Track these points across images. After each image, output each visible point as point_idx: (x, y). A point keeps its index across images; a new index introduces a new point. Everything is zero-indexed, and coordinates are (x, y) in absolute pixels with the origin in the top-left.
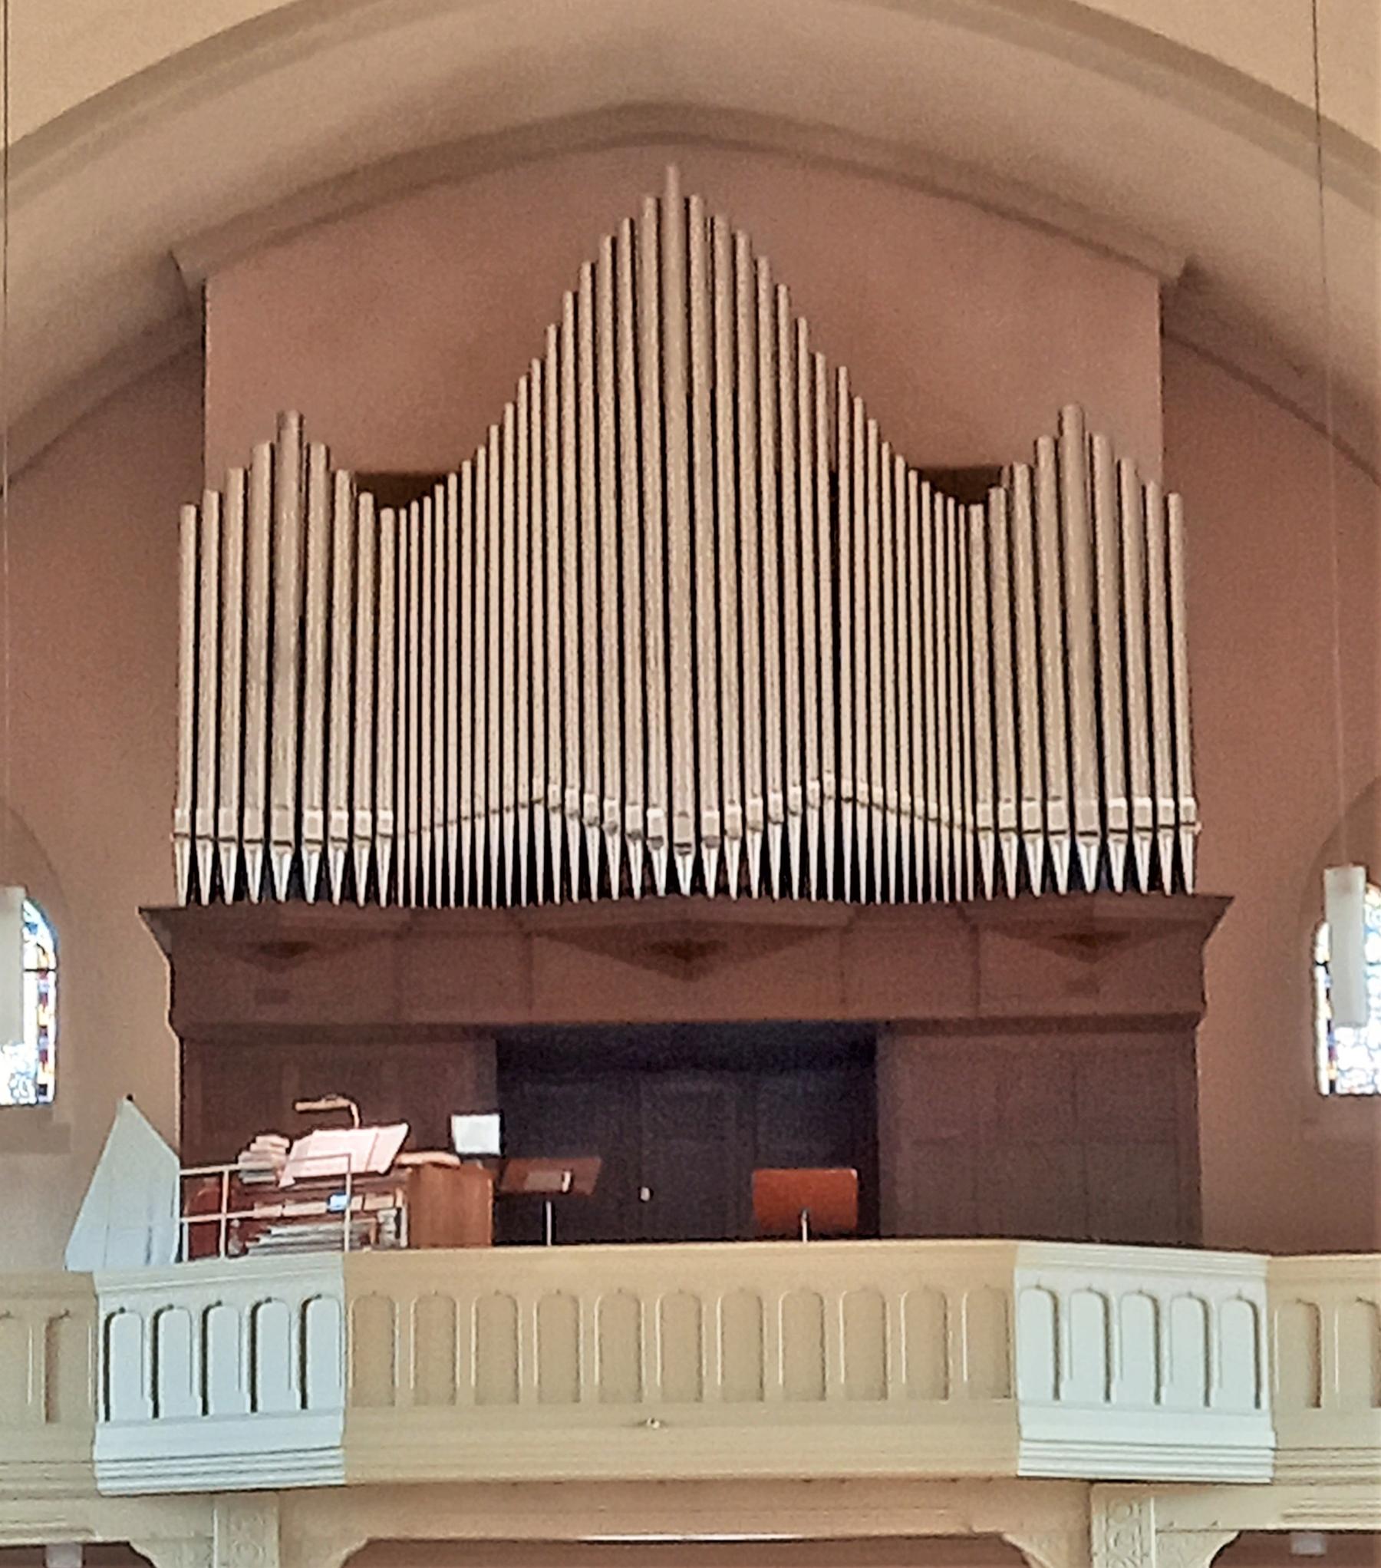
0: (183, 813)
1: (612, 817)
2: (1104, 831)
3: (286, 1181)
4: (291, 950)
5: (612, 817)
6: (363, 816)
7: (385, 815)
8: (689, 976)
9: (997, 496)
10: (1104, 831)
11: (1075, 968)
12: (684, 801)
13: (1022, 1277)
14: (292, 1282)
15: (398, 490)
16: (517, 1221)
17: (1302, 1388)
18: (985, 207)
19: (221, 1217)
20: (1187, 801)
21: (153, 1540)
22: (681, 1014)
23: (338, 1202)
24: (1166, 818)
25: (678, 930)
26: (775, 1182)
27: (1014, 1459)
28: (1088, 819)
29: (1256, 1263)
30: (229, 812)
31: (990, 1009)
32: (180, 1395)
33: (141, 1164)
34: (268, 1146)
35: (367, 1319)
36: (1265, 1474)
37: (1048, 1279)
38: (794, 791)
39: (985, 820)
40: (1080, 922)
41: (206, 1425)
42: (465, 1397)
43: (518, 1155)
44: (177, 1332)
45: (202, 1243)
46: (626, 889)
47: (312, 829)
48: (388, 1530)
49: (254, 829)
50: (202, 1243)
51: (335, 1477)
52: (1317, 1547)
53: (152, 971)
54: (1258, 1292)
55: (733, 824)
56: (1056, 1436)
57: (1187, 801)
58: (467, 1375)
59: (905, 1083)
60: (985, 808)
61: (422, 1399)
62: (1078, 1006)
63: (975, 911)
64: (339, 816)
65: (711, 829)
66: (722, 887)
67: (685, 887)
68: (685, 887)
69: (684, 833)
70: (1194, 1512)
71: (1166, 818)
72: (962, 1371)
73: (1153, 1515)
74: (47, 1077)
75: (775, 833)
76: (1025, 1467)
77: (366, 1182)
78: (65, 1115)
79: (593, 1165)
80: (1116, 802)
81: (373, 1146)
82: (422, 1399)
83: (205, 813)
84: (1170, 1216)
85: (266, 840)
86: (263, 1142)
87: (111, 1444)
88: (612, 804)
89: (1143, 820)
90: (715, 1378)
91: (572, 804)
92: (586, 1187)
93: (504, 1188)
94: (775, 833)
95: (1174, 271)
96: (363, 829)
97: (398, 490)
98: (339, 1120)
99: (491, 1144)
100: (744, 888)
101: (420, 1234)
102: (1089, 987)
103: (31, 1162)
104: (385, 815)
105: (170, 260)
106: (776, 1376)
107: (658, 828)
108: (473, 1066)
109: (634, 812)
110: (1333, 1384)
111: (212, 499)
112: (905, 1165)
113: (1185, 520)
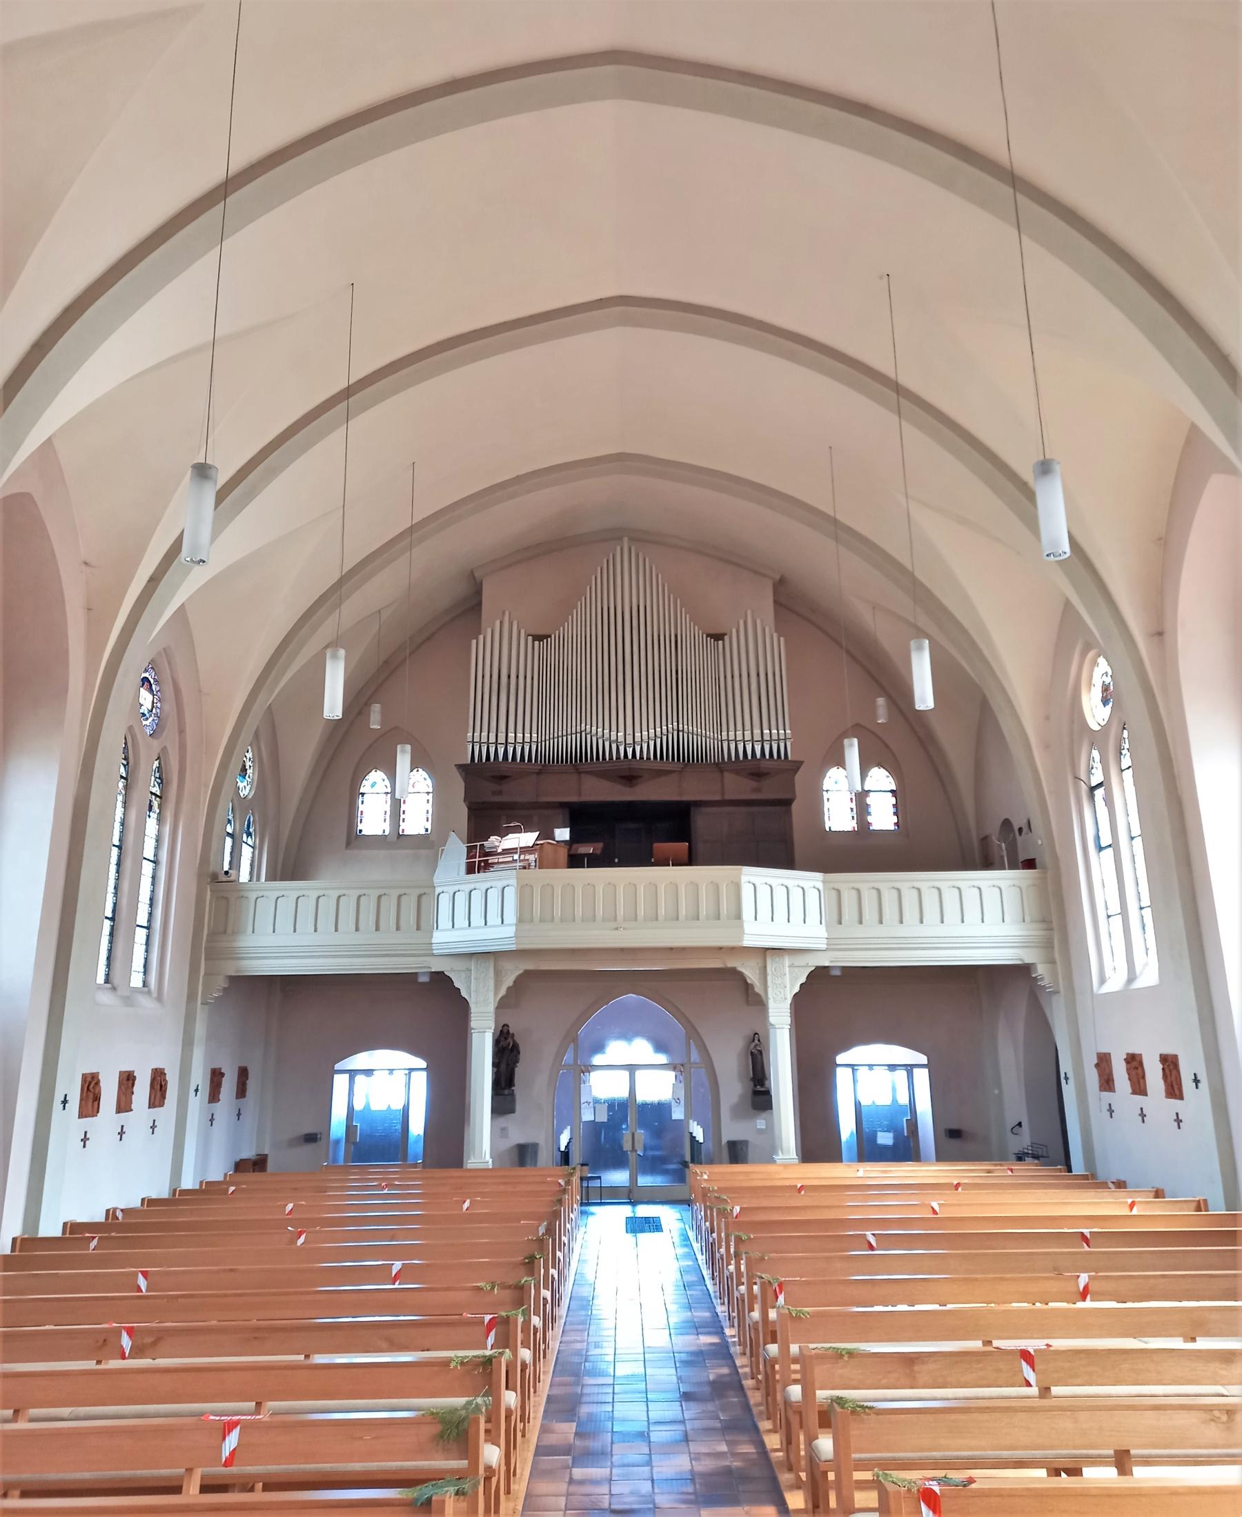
0: (470, 734)
1: (606, 736)
2: (763, 741)
3: (500, 850)
4: (502, 778)
5: (606, 736)
7: (534, 735)
8: (631, 786)
9: (726, 638)
10: (763, 741)
11: (754, 784)
12: (629, 731)
13: (744, 879)
14: (501, 886)
15: (539, 638)
16: (575, 861)
17: (835, 918)
18: (721, 559)
19: (479, 862)
20: (788, 731)
21: (452, 970)
23: (516, 857)
24: (782, 737)
25: (628, 772)
26: (660, 847)
27: (741, 939)
28: (757, 737)
30: (484, 734)
31: (727, 797)
32: (461, 920)
33: (456, 851)
34: (493, 839)
35: (524, 894)
36: (824, 947)
37: (753, 879)
40: (752, 769)
41: (469, 931)
42: (557, 919)
43: (578, 842)
44: (461, 899)
45: (470, 869)
46: (611, 758)
47: (511, 740)
48: (530, 966)
49: (492, 739)
50: (470, 869)
51: (513, 947)
52: (838, 973)
53: (458, 786)
54: (820, 885)
55: (645, 738)
56: (755, 933)
57: (788, 731)
58: (558, 912)
59: (701, 822)
60: (724, 734)
61: (542, 920)
63: (721, 767)
64: (520, 735)
65: (638, 739)
66: (641, 758)
67: (630, 756)
68: (630, 756)
69: (629, 740)
70: (800, 960)
71: (782, 737)
72: (724, 910)
73: (787, 961)
74: (429, 826)
75: (658, 741)
76: (747, 942)
77: (525, 850)
78: (432, 838)
79: (600, 845)
80: (766, 731)
81: (528, 838)
82: (542, 920)
87: (438, 937)
88: (607, 731)
89: (775, 737)
90: (641, 913)
91: (594, 731)
92: (598, 852)
93: (572, 852)
94: (658, 741)
97: (539, 638)
98: (517, 830)
99: (567, 837)
100: (648, 758)
101: (541, 864)
102: (758, 790)
103: (423, 852)
104: (534, 735)
106: (662, 912)
107: (621, 739)
108: (561, 815)
110: (846, 918)
112: (700, 847)
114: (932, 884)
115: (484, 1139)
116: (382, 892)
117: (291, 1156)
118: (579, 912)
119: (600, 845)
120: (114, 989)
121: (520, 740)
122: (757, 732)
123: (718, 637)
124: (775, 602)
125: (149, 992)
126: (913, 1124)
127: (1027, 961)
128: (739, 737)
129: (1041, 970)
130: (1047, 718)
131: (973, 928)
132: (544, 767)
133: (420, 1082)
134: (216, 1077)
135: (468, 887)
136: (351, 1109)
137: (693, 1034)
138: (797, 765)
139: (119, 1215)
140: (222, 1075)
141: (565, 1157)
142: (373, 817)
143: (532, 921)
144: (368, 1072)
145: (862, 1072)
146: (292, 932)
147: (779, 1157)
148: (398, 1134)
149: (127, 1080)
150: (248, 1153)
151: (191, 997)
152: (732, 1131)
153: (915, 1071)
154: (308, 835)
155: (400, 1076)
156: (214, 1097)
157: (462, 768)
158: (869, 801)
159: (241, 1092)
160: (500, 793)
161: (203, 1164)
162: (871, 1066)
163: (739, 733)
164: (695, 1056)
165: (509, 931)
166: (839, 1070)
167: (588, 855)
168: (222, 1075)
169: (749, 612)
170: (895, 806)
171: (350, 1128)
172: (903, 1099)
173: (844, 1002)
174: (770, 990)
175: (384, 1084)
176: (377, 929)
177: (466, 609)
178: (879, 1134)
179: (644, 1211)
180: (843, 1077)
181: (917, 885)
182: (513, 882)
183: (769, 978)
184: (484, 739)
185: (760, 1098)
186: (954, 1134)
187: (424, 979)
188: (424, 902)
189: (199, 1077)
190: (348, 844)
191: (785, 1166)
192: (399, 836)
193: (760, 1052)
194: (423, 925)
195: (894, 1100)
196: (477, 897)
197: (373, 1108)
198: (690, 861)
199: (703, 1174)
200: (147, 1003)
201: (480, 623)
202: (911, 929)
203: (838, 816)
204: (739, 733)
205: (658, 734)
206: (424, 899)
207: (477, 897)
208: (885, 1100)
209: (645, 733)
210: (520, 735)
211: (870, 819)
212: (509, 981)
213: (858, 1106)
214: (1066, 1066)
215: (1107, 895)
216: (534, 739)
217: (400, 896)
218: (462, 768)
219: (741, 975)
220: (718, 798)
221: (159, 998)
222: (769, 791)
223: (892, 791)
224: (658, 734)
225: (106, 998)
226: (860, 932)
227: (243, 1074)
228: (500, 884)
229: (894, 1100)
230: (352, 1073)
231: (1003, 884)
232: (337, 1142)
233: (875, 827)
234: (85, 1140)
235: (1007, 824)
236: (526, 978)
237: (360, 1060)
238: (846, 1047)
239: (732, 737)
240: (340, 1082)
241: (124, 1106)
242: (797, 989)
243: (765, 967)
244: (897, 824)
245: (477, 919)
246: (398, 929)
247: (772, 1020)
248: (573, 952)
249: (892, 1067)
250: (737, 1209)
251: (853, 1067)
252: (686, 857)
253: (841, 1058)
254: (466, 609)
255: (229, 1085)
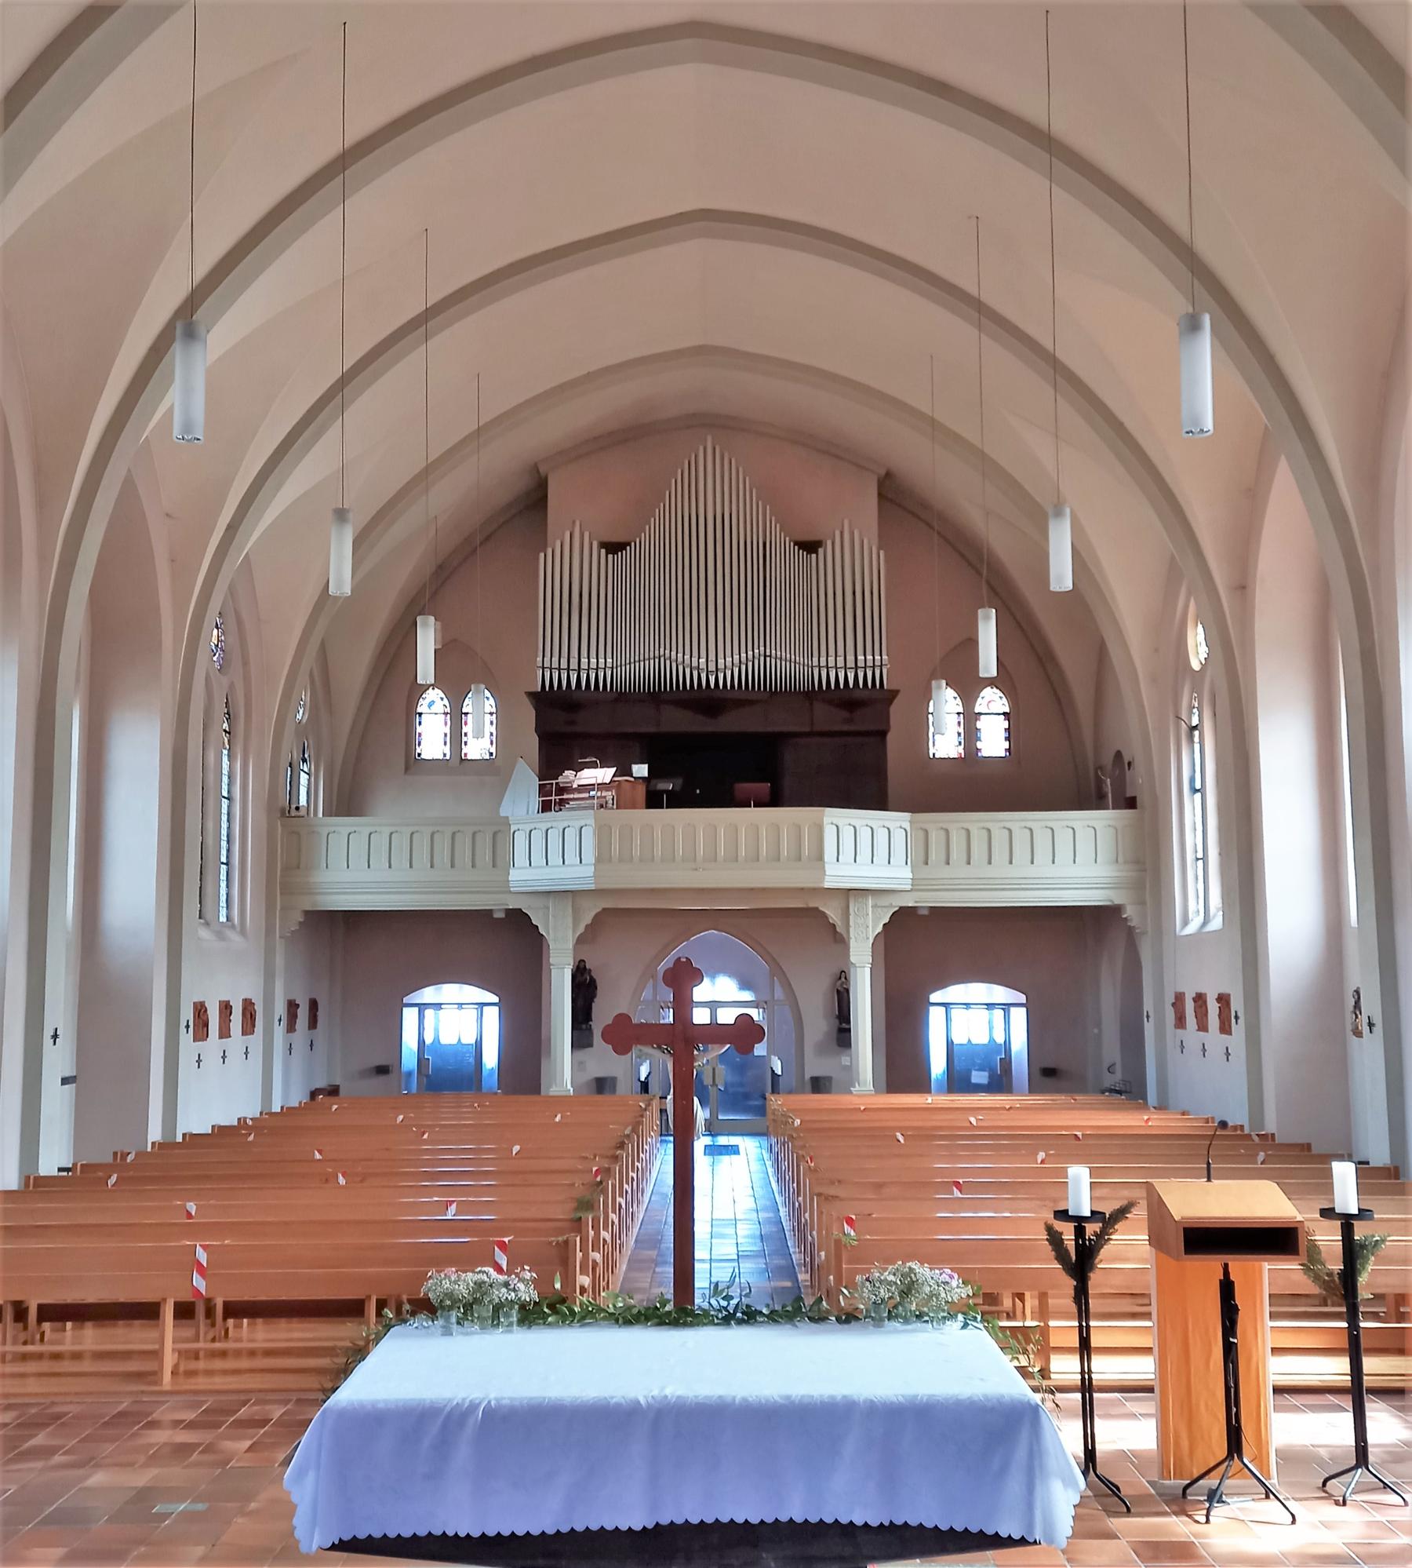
0: (540, 659)
1: (687, 661)
5: (687, 661)
6: (602, 661)
7: (609, 660)
9: (821, 551)
11: (845, 714)
12: (712, 657)
13: (826, 820)
15: (614, 548)
16: (654, 800)
17: (922, 858)
19: (553, 799)
20: (885, 657)
22: (710, 729)
24: (878, 663)
25: (708, 701)
26: (743, 788)
28: (851, 663)
29: (907, 815)
30: (555, 659)
31: (817, 728)
32: (538, 857)
33: (526, 781)
34: (569, 774)
36: (909, 887)
38: (750, 653)
39: (815, 663)
45: (546, 807)
47: (584, 666)
49: (564, 665)
50: (546, 807)
51: (592, 887)
52: (926, 912)
53: (529, 714)
54: (907, 825)
55: (729, 664)
58: (636, 852)
60: (815, 659)
61: (621, 860)
62: (845, 728)
63: (813, 695)
64: (593, 661)
65: (721, 666)
69: (712, 667)
70: (885, 901)
71: (878, 663)
74: (493, 750)
75: (743, 667)
77: (602, 786)
79: (680, 781)
80: (861, 658)
81: (605, 774)
82: (621, 860)
83: (547, 659)
84: (878, 801)
85: (568, 669)
86: (567, 773)
87: (515, 875)
88: (687, 657)
89: (870, 663)
93: (651, 788)
94: (743, 667)
95: (883, 472)
96: (602, 665)
97: (614, 548)
98: (594, 765)
102: (850, 721)
105: (535, 468)
107: (703, 666)
109: (695, 660)
110: (933, 857)
111: (549, 551)
112: (788, 783)
113: (886, 561)
114: (1023, 824)
115: (564, 1069)
116: (456, 829)
117: (366, 1087)
118: (658, 852)
119: (680, 781)
120: (207, 924)
121: (593, 665)
122: (851, 658)
123: (810, 547)
124: (880, 495)
125: (233, 926)
126: (1007, 1063)
127: (1116, 902)
128: (831, 664)
129: (1129, 912)
130: (1156, 650)
131: (1065, 869)
132: (622, 698)
133: (492, 1015)
134: (292, 1007)
135: (544, 827)
136: (421, 1042)
137: (777, 971)
138: (893, 694)
139: (250, 1123)
140: (298, 1006)
141: (645, 1087)
142: (432, 741)
143: (610, 860)
144: (438, 1006)
145: (955, 1013)
146: (366, 867)
147: (856, 1089)
148: (472, 1068)
149: (226, 1008)
150: (321, 1083)
151: (269, 931)
152: (814, 1067)
153: (1012, 1009)
154: (365, 758)
155: (472, 1013)
156: (291, 1028)
157: (532, 696)
158: (979, 725)
159: (313, 1023)
160: (572, 723)
161: (287, 1094)
162: (967, 1005)
163: (831, 659)
164: (779, 993)
165: (590, 871)
166: (932, 1009)
167: (667, 792)
168: (298, 1006)
169: (846, 522)
170: (1008, 730)
171: (421, 1061)
172: (1000, 1040)
173: (931, 943)
174: (851, 930)
175: (456, 1017)
176: (452, 866)
177: (532, 502)
178: (974, 1073)
179: (723, 1140)
180: (936, 1015)
181: (1008, 825)
182: (591, 822)
183: (851, 918)
184: (555, 665)
185: (842, 1034)
186: (1049, 1072)
187: (502, 915)
188: (498, 840)
189: (280, 1009)
190: (407, 769)
191: (859, 1096)
192: (463, 761)
193: (847, 991)
194: (499, 862)
195: (992, 1040)
196: (554, 837)
197: (443, 1041)
198: (775, 800)
199: (776, 1102)
200: (234, 936)
201: (546, 525)
202: (1000, 869)
203: (945, 744)
204: (831, 659)
205: (743, 659)
206: (499, 835)
207: (554, 837)
208: (981, 1039)
209: (729, 659)
210: (593, 661)
211: (979, 745)
212: (587, 918)
213: (950, 1045)
214: (1148, 1005)
215: (1193, 840)
216: (609, 665)
217: (474, 834)
218: (532, 696)
219: (824, 915)
220: (807, 729)
221: (243, 932)
222: (864, 721)
223: (1004, 714)
224: (743, 659)
225: (204, 933)
226: (946, 872)
227: (314, 1005)
228: (578, 824)
229: (992, 1040)
230: (422, 1007)
231: (1098, 825)
232: (409, 1074)
233: (985, 753)
234: (199, 1061)
235: (1119, 755)
236: (603, 918)
237: (428, 994)
238: (942, 984)
239: (823, 663)
240: (410, 1016)
241: (225, 1033)
242: (880, 929)
243: (848, 907)
244: (1008, 750)
245: (555, 858)
246: (473, 866)
247: (853, 959)
248: (652, 890)
249: (990, 1006)
250: (798, 1122)
251: (945, 1005)
252: (767, 799)
253: (935, 997)
254: (532, 502)
255: (303, 1014)
